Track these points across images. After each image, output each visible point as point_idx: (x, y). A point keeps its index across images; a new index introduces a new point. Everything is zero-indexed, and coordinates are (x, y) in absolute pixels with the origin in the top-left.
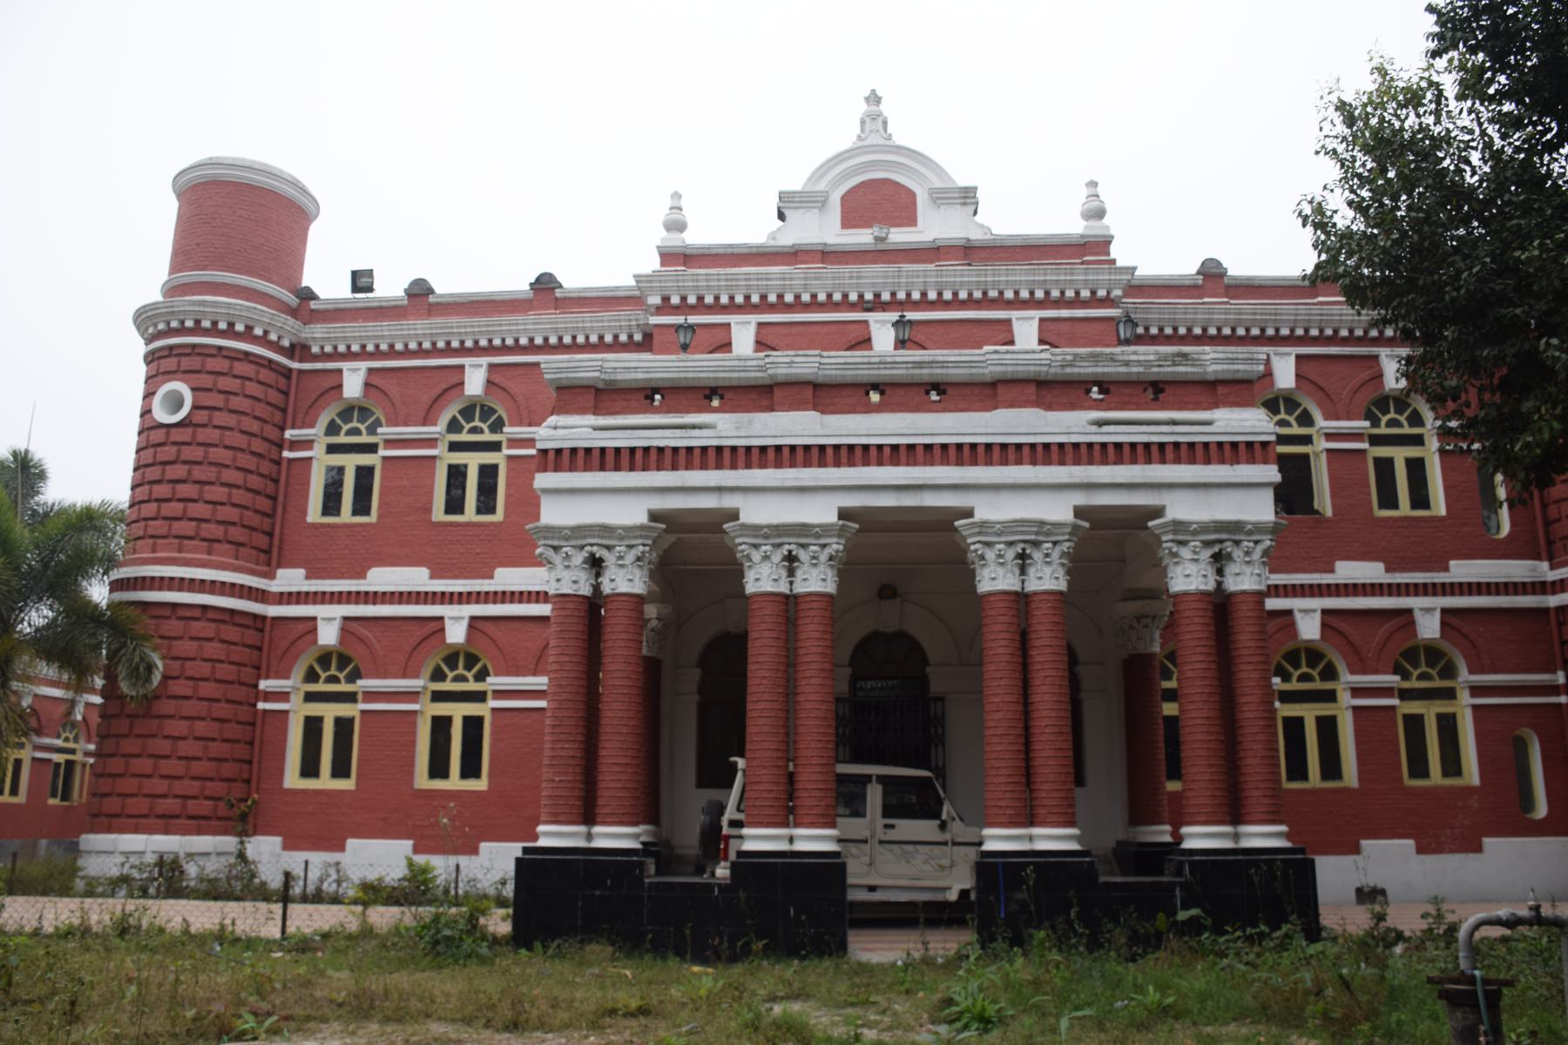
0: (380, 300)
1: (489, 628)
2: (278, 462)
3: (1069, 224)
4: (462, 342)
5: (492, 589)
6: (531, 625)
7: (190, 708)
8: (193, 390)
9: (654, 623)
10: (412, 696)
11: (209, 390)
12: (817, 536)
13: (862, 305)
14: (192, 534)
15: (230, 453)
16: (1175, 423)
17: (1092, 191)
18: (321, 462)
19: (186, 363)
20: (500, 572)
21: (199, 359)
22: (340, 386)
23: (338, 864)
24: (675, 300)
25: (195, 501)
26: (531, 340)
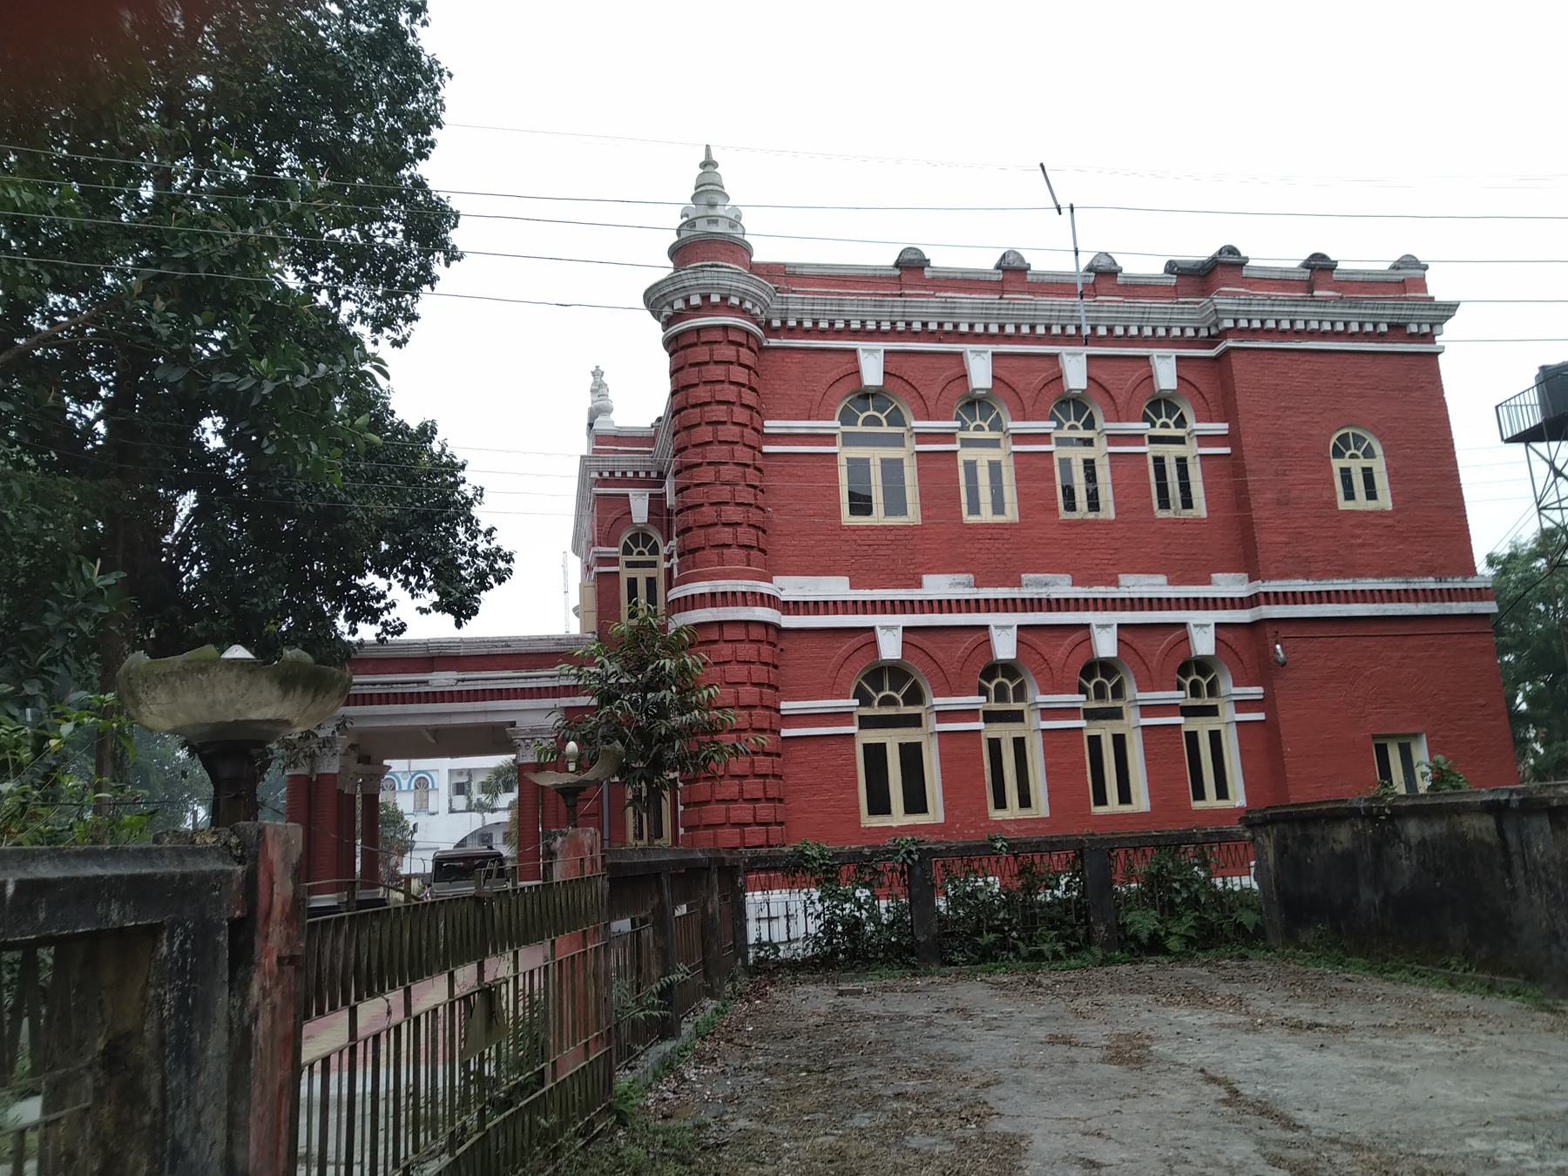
20: (927, 579)
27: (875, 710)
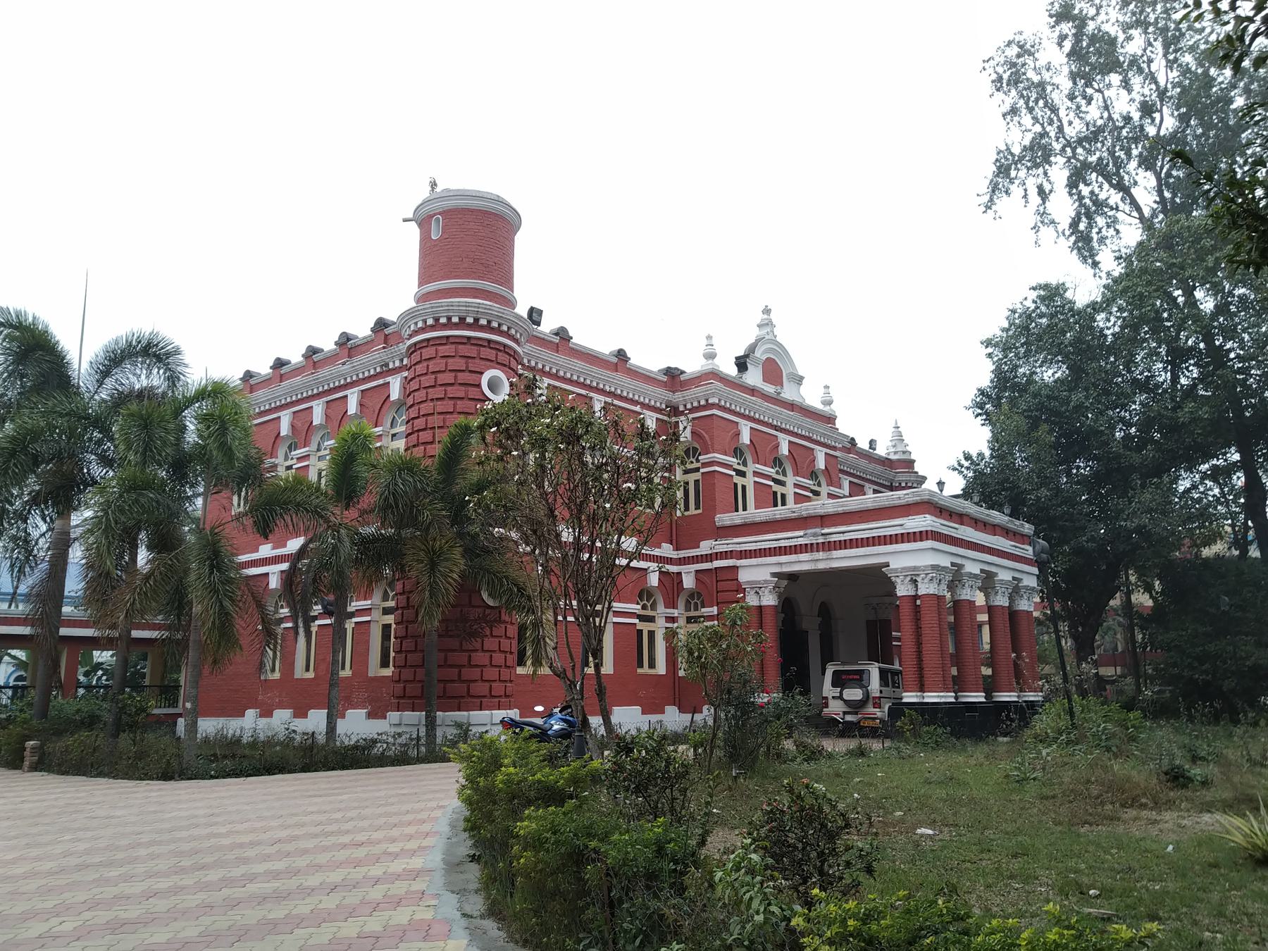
13: (776, 428)
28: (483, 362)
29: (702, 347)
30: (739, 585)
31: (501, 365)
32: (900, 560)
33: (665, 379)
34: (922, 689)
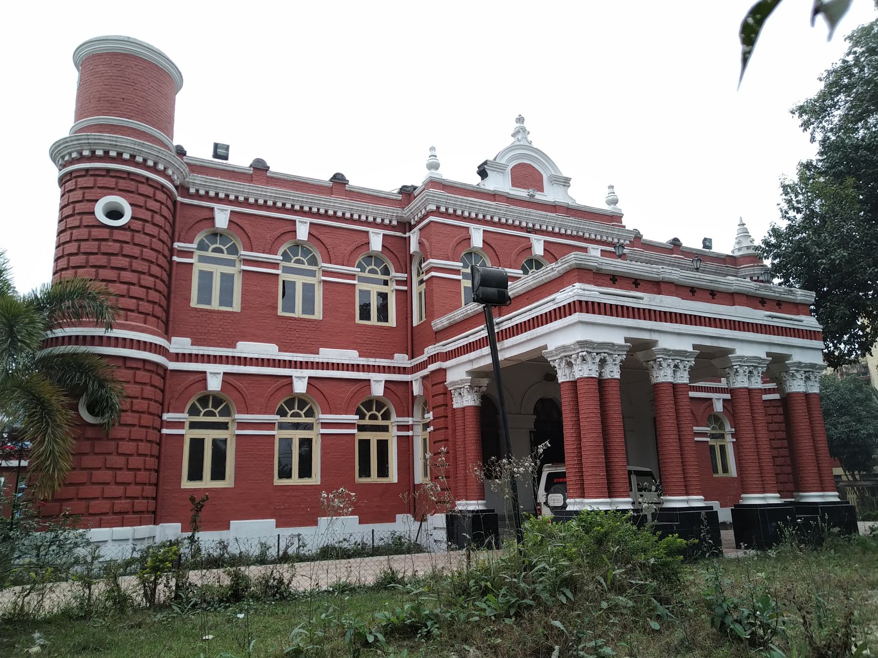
0: (229, 166)
1: (318, 384)
2: (171, 262)
3: (599, 203)
4: (293, 206)
5: (321, 361)
6: (343, 384)
7: (138, 433)
8: (131, 205)
9: (484, 389)
10: (270, 425)
11: (141, 207)
12: (686, 357)
13: (527, 230)
14: (134, 308)
15: (154, 254)
16: (791, 319)
17: (611, 190)
18: (198, 266)
19: (122, 184)
21: (114, 180)
22: (213, 219)
23: (299, 535)
24: (443, 209)
25: (134, 284)
26: (335, 213)
27: (367, 422)
28: (99, 191)
29: (425, 160)
30: (446, 388)
31: (123, 192)
32: (558, 338)
33: (400, 197)
34: (611, 493)
